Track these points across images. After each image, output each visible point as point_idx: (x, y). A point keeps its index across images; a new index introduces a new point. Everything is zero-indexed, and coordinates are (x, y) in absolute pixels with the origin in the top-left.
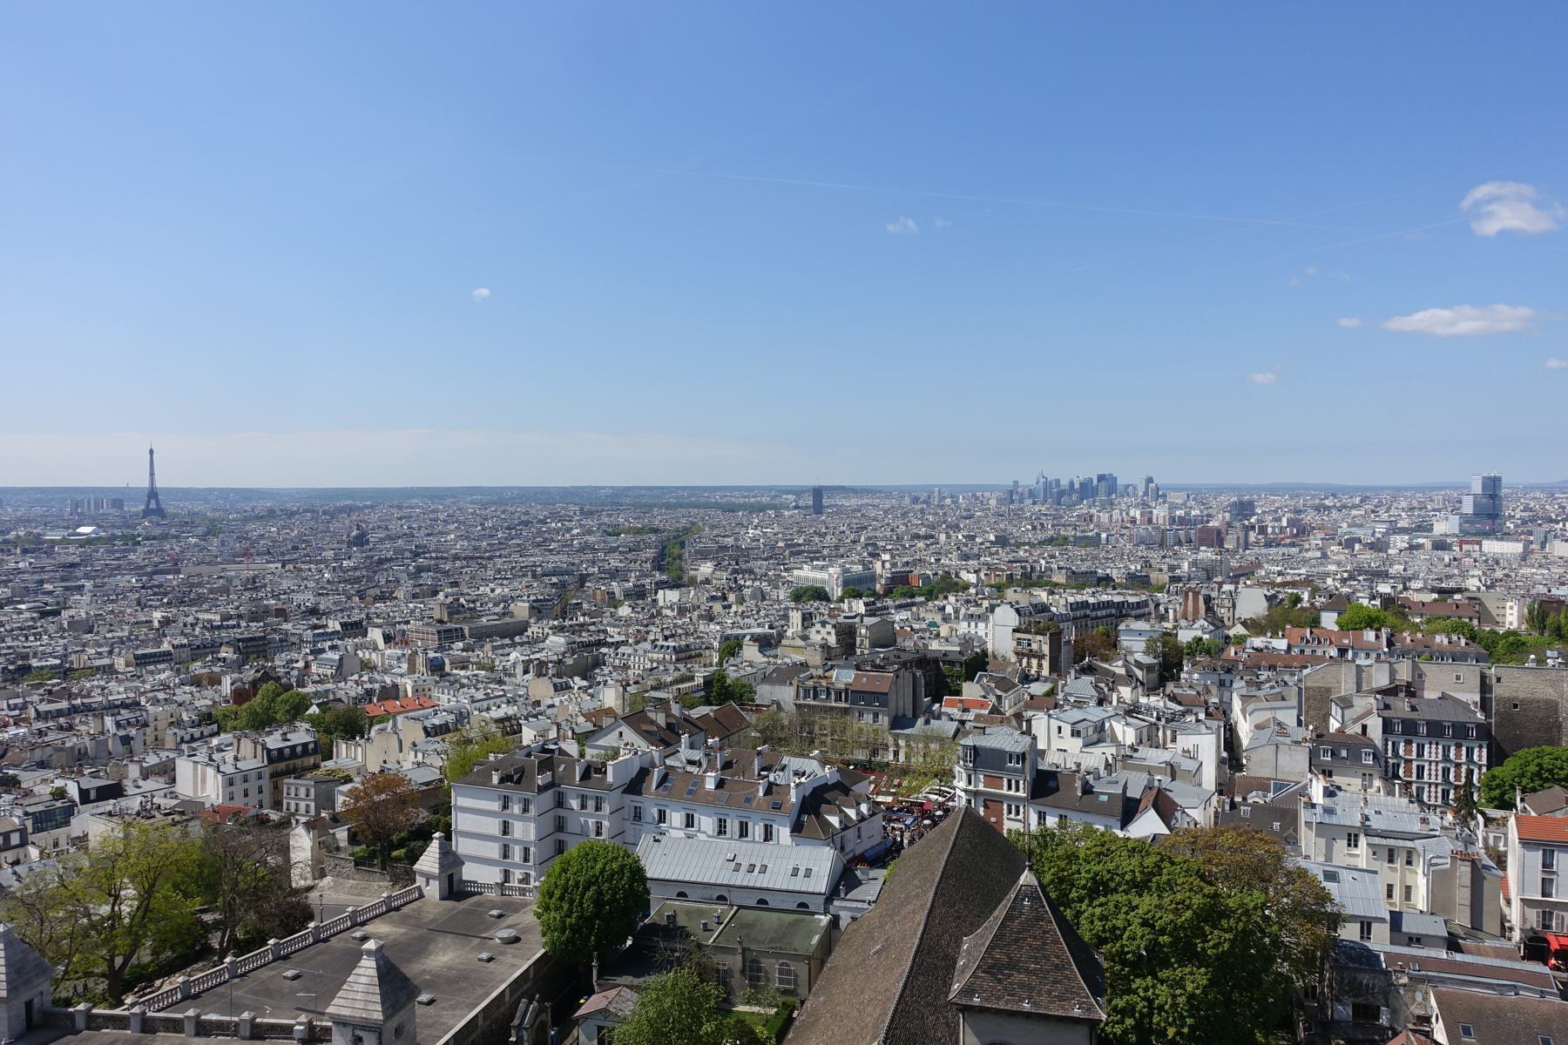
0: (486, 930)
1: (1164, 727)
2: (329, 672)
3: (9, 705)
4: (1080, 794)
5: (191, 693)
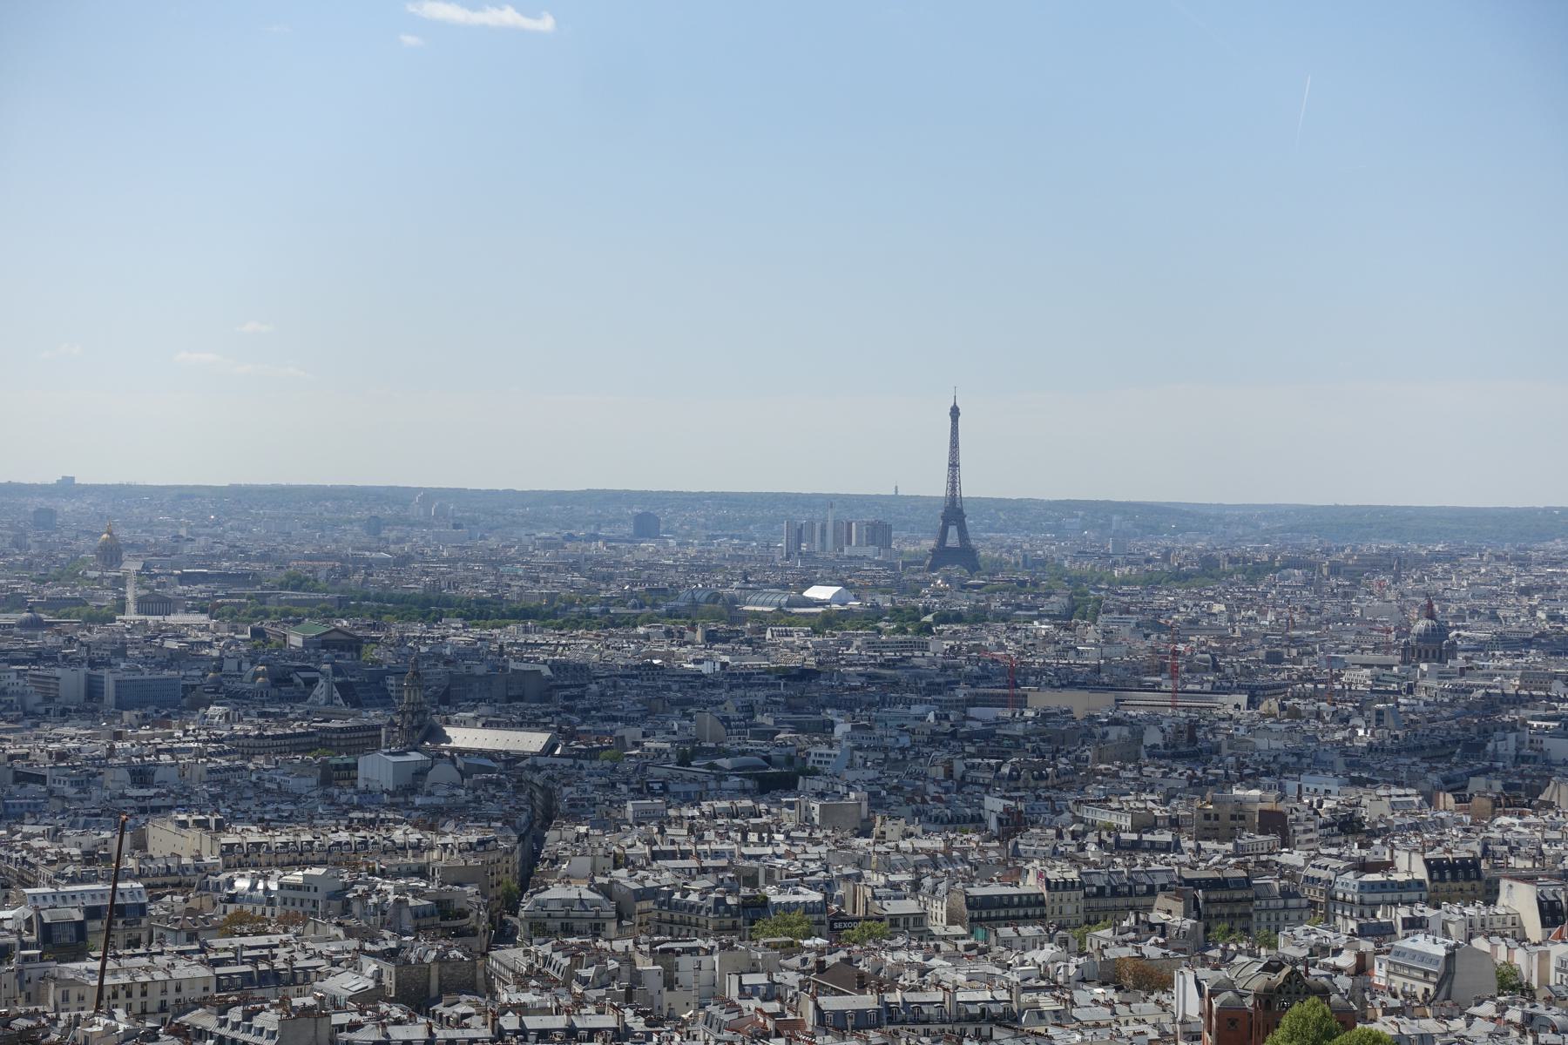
2: (1419, 988)
3: (741, 986)
5: (1109, 1004)
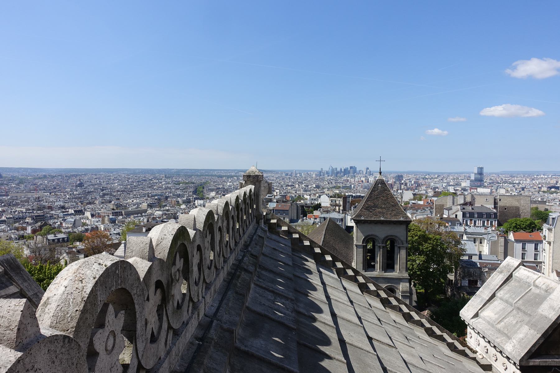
2: (70, 226)
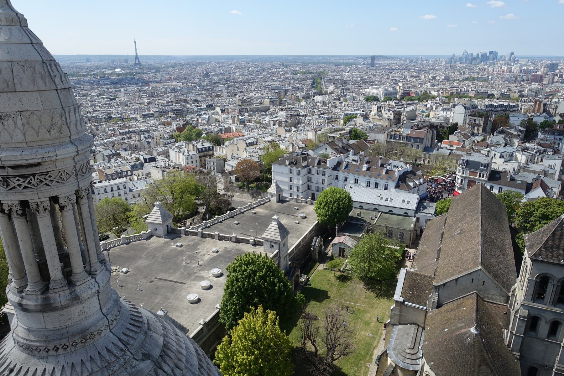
0: (294, 213)
1: (538, 156)
2: (205, 122)
4: (509, 180)
5: (163, 128)
